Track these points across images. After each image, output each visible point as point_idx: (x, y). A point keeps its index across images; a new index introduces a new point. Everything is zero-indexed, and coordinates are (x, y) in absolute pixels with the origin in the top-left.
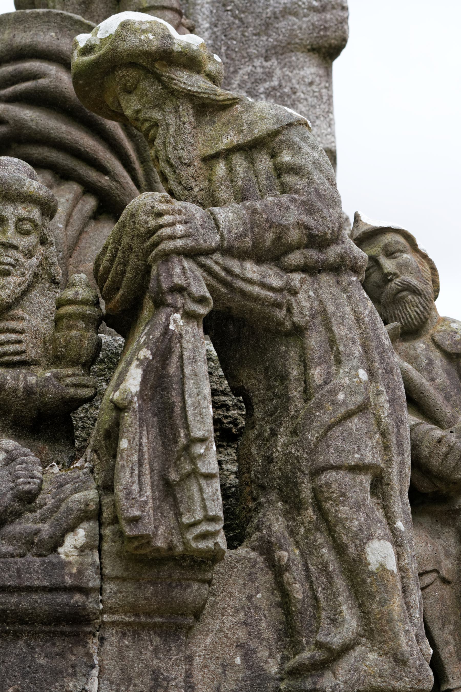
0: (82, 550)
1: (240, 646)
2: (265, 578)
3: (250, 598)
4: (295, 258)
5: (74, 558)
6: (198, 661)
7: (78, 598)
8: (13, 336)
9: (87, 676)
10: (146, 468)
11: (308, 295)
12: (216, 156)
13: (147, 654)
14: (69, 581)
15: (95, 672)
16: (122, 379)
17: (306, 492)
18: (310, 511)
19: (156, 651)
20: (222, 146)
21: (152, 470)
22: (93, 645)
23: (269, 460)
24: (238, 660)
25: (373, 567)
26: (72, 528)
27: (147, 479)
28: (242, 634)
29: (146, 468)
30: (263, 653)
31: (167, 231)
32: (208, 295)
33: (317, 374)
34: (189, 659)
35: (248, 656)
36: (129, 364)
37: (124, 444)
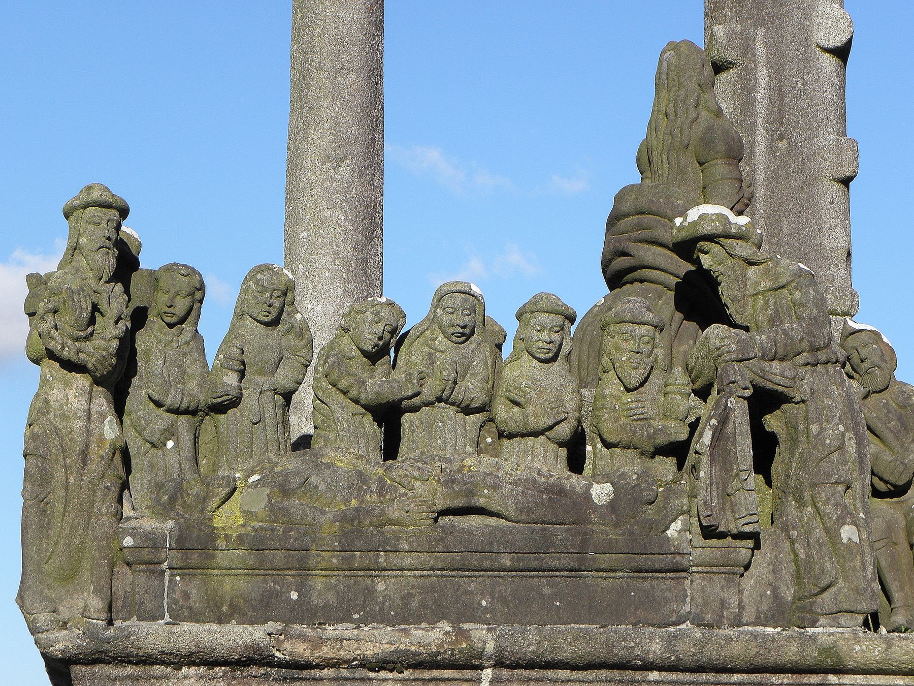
0: (680, 532)
1: (770, 584)
2: (787, 544)
3: (776, 557)
4: (800, 359)
5: (676, 535)
6: (746, 593)
7: (678, 558)
8: (640, 405)
9: (684, 602)
10: (714, 488)
11: (808, 382)
12: (759, 293)
13: (717, 589)
14: (672, 549)
15: (688, 600)
16: (701, 435)
17: (807, 496)
18: (810, 508)
19: (722, 588)
20: (760, 288)
21: (718, 488)
22: (687, 583)
23: (788, 476)
24: (769, 592)
25: (845, 541)
26: (674, 520)
27: (715, 493)
28: (771, 578)
29: (714, 488)
30: (783, 588)
31: (725, 349)
32: (750, 386)
33: (814, 428)
34: (741, 592)
35: (775, 590)
36: (705, 428)
37: (702, 474)
